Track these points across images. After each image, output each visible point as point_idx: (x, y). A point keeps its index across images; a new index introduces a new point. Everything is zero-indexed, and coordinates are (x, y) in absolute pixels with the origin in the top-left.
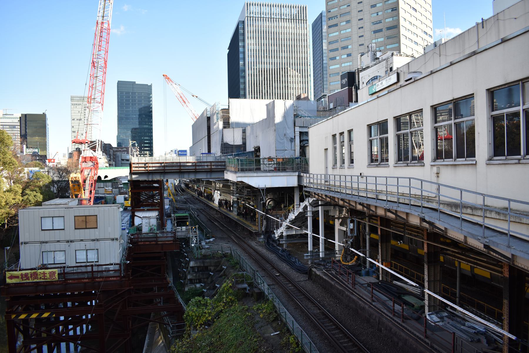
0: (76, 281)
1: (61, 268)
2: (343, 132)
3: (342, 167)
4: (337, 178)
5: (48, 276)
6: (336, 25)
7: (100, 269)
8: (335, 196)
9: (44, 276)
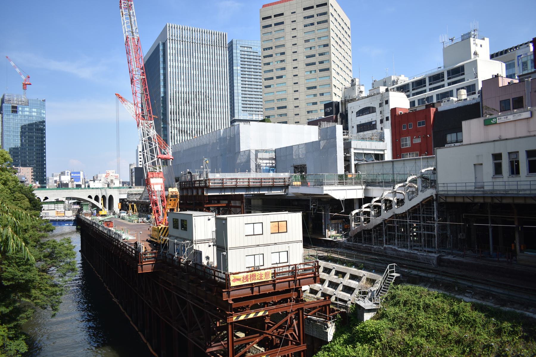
5: (264, 276)
6: (271, 56)
9: (261, 277)
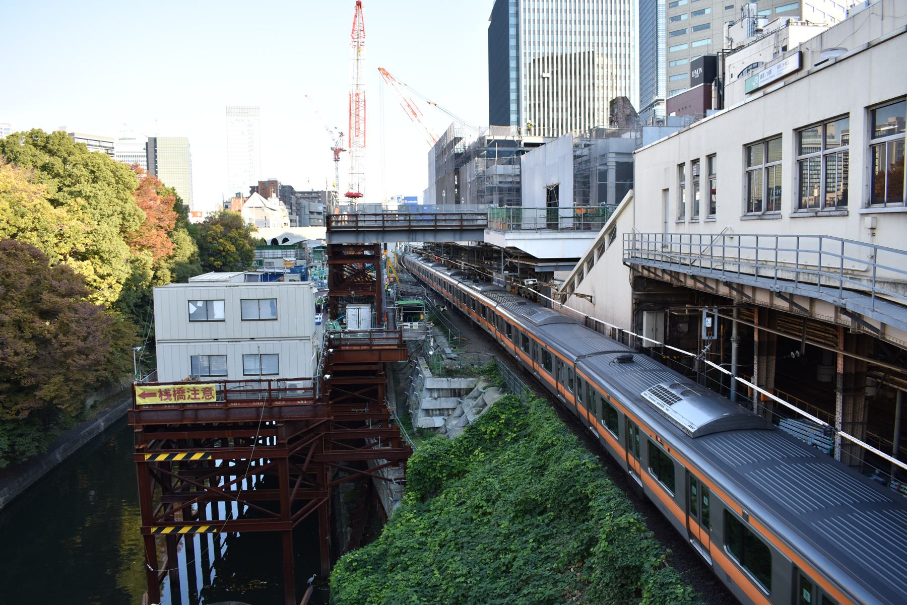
0: (244, 405)
1: (220, 382)
2: (698, 160)
3: (693, 221)
4: (686, 239)
7: (282, 385)
8: (681, 271)
9: (195, 394)
